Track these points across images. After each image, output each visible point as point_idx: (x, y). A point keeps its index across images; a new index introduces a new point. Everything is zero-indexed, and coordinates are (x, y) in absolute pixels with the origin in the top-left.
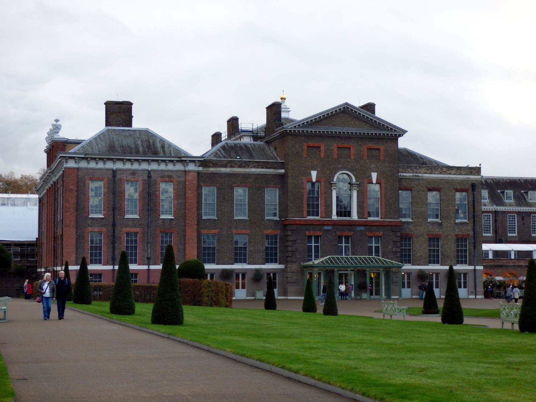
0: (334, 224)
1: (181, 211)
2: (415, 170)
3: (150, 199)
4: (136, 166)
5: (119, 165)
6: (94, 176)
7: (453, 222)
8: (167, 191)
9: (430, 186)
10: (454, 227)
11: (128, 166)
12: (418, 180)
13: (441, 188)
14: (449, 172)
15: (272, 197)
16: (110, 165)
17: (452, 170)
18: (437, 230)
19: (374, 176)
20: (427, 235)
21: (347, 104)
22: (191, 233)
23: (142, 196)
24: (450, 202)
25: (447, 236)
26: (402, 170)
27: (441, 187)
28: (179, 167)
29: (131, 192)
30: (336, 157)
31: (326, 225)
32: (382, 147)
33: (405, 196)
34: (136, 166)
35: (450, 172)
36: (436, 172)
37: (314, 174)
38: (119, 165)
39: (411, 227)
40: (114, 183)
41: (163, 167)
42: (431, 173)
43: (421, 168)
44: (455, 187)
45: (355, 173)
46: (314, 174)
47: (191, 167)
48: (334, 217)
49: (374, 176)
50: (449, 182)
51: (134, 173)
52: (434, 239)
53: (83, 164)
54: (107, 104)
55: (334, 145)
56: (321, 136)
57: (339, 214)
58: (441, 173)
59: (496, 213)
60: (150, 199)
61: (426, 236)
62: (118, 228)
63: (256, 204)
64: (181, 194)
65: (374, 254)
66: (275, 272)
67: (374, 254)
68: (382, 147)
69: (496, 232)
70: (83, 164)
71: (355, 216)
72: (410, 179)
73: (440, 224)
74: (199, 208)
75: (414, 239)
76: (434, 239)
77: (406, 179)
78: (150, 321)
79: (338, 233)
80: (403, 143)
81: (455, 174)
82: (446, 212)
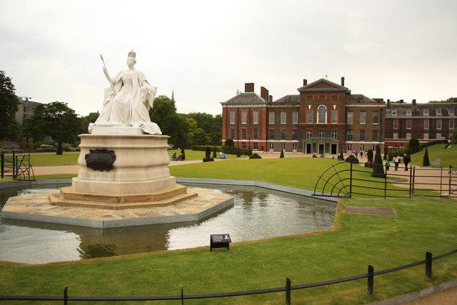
0: (318, 125)
1: (260, 122)
3: (250, 118)
4: (246, 106)
5: (240, 106)
6: (232, 109)
8: (256, 115)
11: (243, 106)
12: (356, 107)
15: (295, 116)
16: (237, 106)
19: (335, 106)
22: (264, 130)
23: (247, 116)
28: (260, 106)
29: (244, 115)
33: (350, 115)
34: (246, 106)
37: (310, 106)
38: (240, 106)
40: (238, 111)
41: (254, 106)
46: (310, 106)
47: (264, 106)
48: (318, 123)
49: (335, 106)
50: (370, 108)
51: (244, 108)
52: (363, 131)
53: (228, 106)
54: (246, 84)
55: (318, 96)
56: (314, 92)
57: (319, 121)
59: (431, 119)
60: (250, 118)
63: (289, 118)
64: (260, 115)
66: (296, 143)
69: (430, 128)
70: (228, 106)
71: (326, 123)
74: (267, 120)
76: (363, 131)
78: (118, 154)
80: (352, 93)
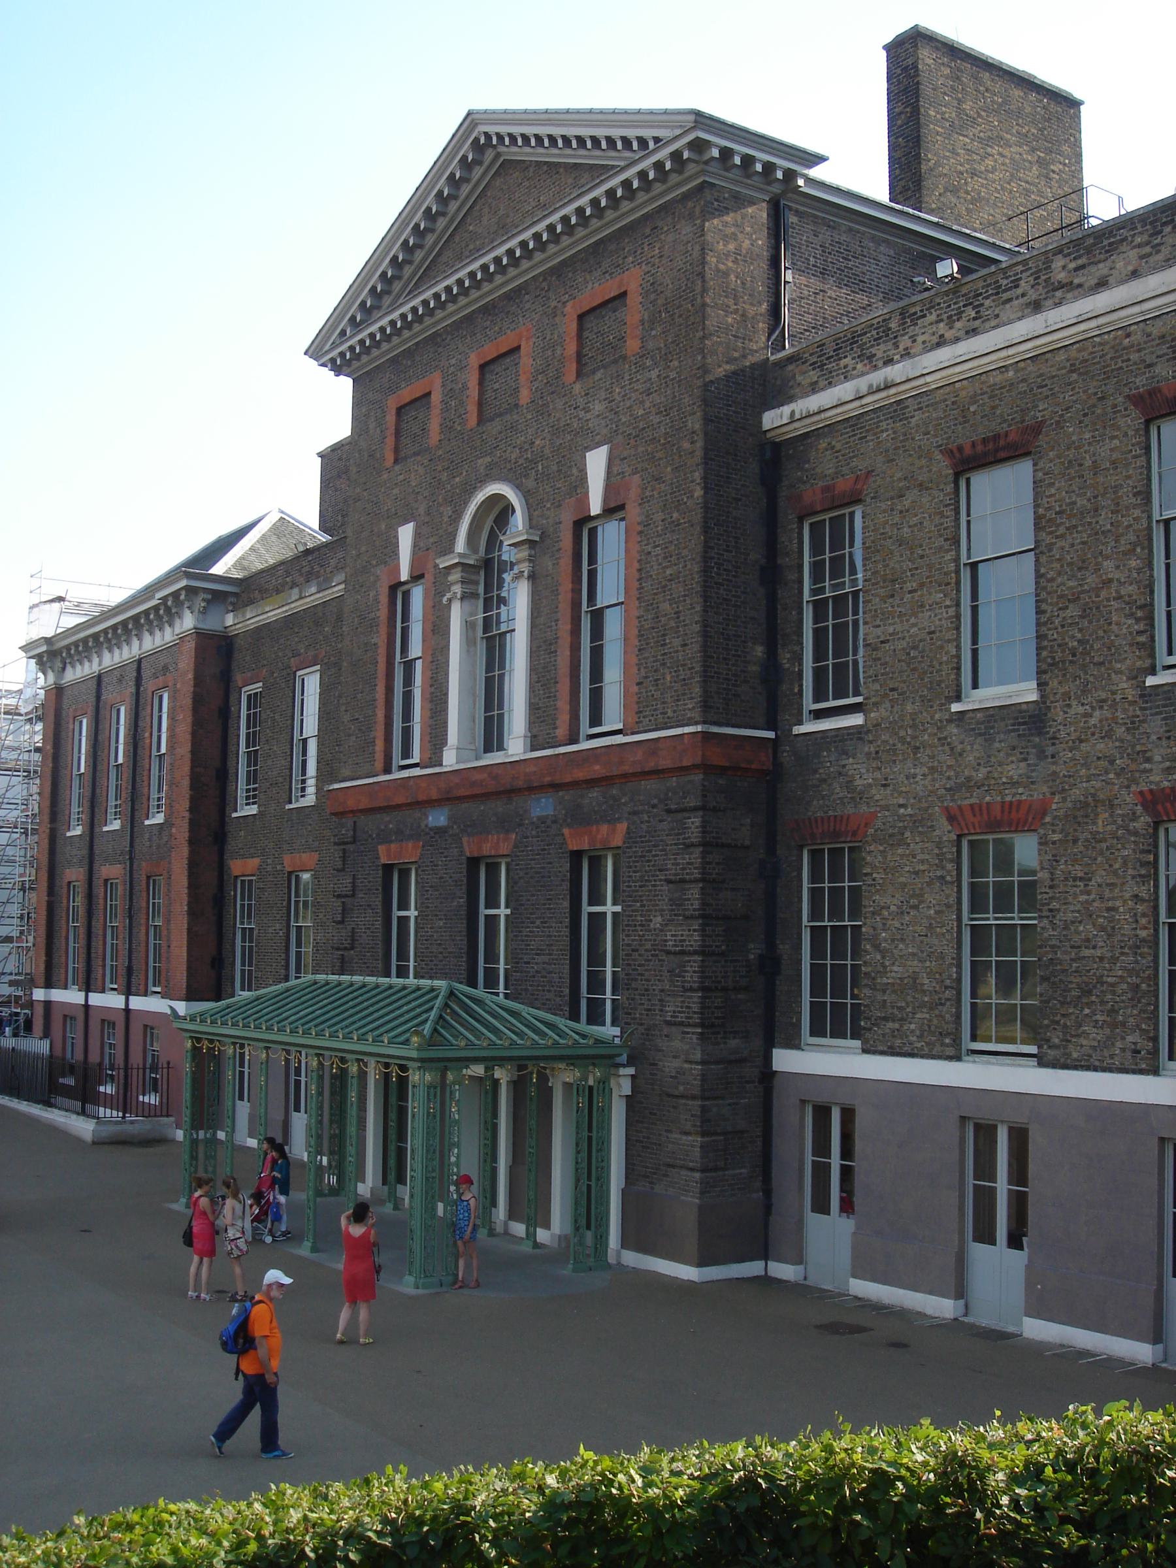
2: (879, 351)
7: (1124, 684)
9: (966, 437)
10: (1133, 725)
13: (1037, 429)
14: (1088, 278)
17: (1111, 249)
18: (1015, 770)
20: (951, 819)
21: (471, 119)
24: (1104, 520)
25: (1085, 809)
26: (813, 375)
27: (1043, 410)
30: (473, 420)
31: (431, 803)
32: (633, 280)
35: (1102, 269)
36: (1008, 312)
39: (861, 772)
42: (972, 332)
43: (915, 318)
44: (1141, 383)
45: (530, 483)
58: (1037, 307)
61: (944, 830)
62: (96, 866)
65: (411, 975)
67: (411, 975)
68: (633, 280)
72: (852, 423)
73: (1030, 722)
75: (873, 855)
77: (831, 428)
79: (469, 847)
81: (1135, 274)
82: (1073, 611)
